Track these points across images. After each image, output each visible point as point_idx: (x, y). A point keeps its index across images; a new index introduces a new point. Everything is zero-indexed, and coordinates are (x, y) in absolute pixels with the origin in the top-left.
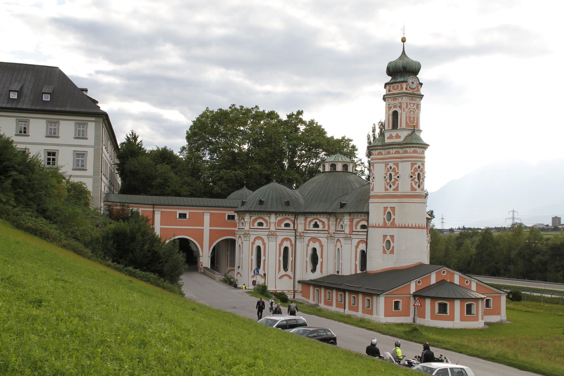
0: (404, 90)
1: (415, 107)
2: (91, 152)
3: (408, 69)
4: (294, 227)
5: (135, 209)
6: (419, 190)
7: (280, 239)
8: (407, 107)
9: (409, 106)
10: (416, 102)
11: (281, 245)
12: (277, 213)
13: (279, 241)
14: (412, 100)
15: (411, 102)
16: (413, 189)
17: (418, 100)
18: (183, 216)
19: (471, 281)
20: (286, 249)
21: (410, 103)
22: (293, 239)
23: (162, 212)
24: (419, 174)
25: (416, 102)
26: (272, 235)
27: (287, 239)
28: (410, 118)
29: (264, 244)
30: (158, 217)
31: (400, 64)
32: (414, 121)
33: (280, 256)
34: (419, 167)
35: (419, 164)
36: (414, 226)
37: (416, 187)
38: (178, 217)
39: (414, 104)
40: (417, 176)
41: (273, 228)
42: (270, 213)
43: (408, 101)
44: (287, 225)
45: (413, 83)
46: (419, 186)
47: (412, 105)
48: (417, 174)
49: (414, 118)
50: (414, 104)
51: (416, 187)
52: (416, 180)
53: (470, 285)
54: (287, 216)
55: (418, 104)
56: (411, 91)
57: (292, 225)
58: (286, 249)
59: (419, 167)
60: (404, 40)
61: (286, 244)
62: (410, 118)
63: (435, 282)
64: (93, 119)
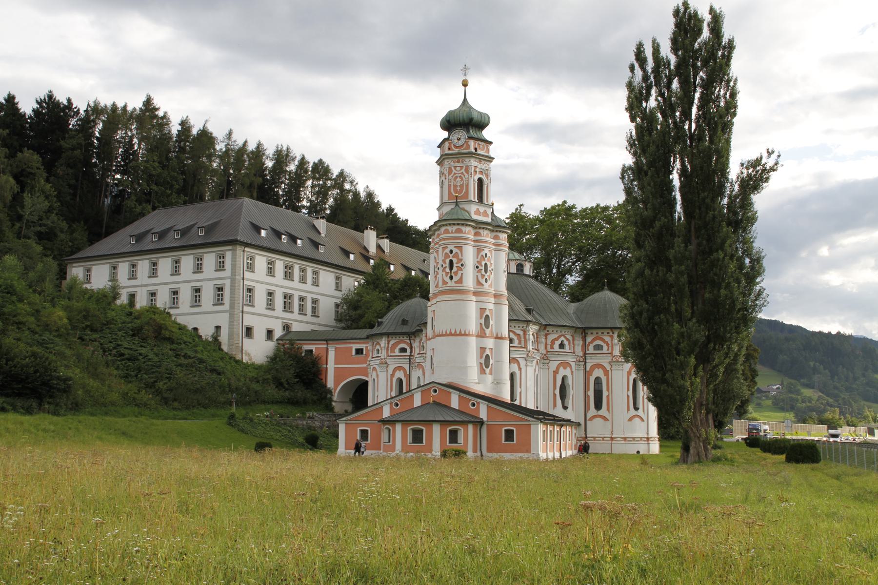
0: (447, 152)
1: (463, 170)
2: (227, 284)
3: (452, 121)
4: (411, 352)
5: (312, 347)
6: (451, 284)
7: (391, 368)
8: (450, 172)
9: (454, 171)
10: (464, 164)
11: (392, 376)
12: (388, 335)
13: (390, 372)
14: (458, 162)
15: (457, 165)
16: (445, 283)
17: (467, 160)
18: (359, 351)
19: (478, 403)
20: (400, 381)
21: (455, 167)
22: (407, 367)
23: (336, 348)
24: (451, 262)
25: (464, 164)
26: (384, 363)
27: (399, 368)
28: (455, 186)
29: (377, 376)
30: (332, 354)
31: (463, 116)
32: (461, 191)
33: (391, 390)
34: (451, 252)
35: (451, 247)
36: (453, 332)
37: (483, 281)
38: (354, 353)
39: (461, 167)
40: (447, 265)
41: (383, 354)
42: (381, 335)
43: (452, 164)
44: (403, 350)
45: (459, 139)
46: (451, 278)
47: (458, 169)
48: (448, 261)
49: (462, 186)
50: (461, 167)
51: (447, 279)
52: (448, 270)
53: (478, 409)
54: (401, 338)
55: (467, 167)
56: (456, 151)
57: (409, 350)
58: (400, 381)
59: (451, 252)
60: (465, 84)
61: (400, 374)
62: (455, 186)
63: (420, 404)
64: (230, 247)
